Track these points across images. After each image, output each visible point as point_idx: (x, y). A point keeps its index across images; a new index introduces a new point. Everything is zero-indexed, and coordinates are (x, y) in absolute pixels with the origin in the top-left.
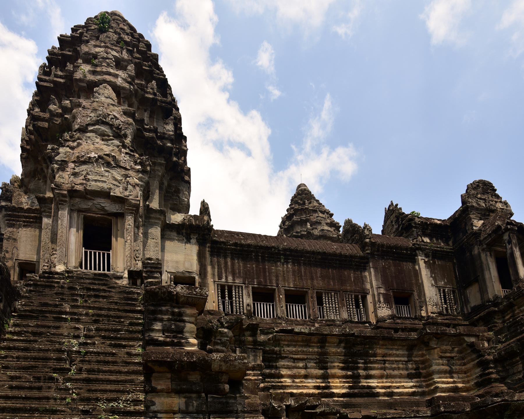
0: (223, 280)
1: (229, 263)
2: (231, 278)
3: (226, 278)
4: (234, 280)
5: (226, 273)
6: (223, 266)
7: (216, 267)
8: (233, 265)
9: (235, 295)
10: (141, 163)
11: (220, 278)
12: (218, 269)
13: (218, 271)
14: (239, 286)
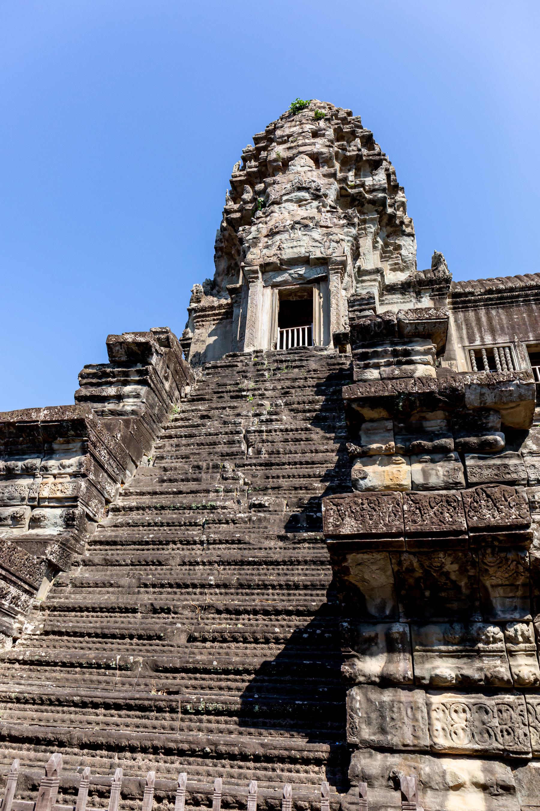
0: (478, 342)
1: (484, 319)
2: (490, 338)
3: (482, 338)
4: (494, 339)
5: (480, 331)
6: (474, 324)
7: (464, 327)
8: (490, 320)
9: (500, 361)
10: (345, 217)
11: (471, 340)
12: (467, 329)
13: (468, 333)
14: (504, 348)
